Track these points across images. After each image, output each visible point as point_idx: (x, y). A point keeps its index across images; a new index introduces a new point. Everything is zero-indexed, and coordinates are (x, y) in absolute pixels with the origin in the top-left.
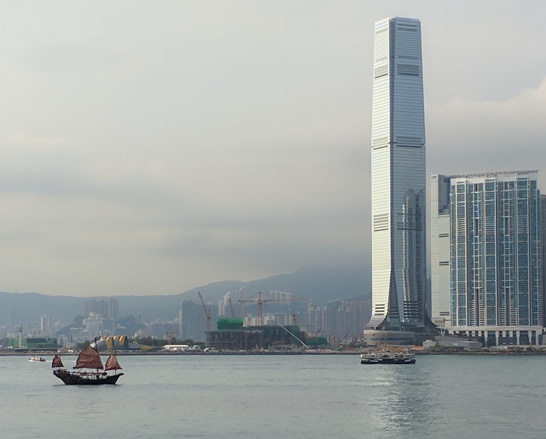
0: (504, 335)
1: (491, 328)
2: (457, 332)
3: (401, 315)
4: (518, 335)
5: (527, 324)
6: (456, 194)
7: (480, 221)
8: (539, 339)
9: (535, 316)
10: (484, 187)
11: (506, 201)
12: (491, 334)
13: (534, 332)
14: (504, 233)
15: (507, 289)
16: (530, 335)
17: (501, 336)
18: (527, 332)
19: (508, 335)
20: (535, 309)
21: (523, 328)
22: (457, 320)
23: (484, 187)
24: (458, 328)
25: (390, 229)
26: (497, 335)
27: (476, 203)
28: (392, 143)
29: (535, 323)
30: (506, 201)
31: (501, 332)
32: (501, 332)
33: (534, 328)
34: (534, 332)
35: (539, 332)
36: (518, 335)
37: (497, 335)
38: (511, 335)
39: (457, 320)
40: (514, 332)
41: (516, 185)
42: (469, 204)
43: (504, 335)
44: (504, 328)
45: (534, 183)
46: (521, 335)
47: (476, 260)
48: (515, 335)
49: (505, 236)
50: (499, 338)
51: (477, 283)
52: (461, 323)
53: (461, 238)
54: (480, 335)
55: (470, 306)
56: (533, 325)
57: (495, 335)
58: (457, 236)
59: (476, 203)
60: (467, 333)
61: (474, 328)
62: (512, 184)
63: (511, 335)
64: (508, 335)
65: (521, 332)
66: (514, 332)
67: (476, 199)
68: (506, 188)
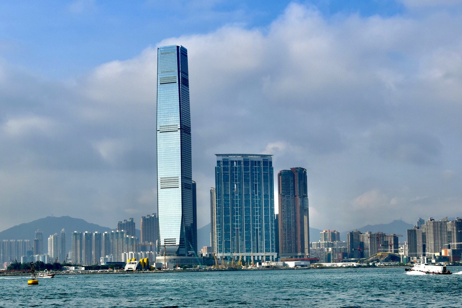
0: (256, 259)
1: (248, 254)
5: (269, 252)
9: (272, 246)
13: (273, 256)
15: (257, 229)
17: (254, 259)
18: (269, 256)
19: (258, 259)
21: (268, 254)
25: (180, 188)
27: (236, 173)
28: (181, 129)
29: (273, 251)
31: (254, 257)
34: (273, 256)
35: (275, 256)
40: (262, 256)
41: (262, 163)
43: (256, 259)
44: (256, 254)
45: (271, 163)
53: (226, 195)
62: (259, 162)
64: (258, 259)
65: (266, 256)
66: (262, 256)
67: (236, 171)
68: (255, 165)
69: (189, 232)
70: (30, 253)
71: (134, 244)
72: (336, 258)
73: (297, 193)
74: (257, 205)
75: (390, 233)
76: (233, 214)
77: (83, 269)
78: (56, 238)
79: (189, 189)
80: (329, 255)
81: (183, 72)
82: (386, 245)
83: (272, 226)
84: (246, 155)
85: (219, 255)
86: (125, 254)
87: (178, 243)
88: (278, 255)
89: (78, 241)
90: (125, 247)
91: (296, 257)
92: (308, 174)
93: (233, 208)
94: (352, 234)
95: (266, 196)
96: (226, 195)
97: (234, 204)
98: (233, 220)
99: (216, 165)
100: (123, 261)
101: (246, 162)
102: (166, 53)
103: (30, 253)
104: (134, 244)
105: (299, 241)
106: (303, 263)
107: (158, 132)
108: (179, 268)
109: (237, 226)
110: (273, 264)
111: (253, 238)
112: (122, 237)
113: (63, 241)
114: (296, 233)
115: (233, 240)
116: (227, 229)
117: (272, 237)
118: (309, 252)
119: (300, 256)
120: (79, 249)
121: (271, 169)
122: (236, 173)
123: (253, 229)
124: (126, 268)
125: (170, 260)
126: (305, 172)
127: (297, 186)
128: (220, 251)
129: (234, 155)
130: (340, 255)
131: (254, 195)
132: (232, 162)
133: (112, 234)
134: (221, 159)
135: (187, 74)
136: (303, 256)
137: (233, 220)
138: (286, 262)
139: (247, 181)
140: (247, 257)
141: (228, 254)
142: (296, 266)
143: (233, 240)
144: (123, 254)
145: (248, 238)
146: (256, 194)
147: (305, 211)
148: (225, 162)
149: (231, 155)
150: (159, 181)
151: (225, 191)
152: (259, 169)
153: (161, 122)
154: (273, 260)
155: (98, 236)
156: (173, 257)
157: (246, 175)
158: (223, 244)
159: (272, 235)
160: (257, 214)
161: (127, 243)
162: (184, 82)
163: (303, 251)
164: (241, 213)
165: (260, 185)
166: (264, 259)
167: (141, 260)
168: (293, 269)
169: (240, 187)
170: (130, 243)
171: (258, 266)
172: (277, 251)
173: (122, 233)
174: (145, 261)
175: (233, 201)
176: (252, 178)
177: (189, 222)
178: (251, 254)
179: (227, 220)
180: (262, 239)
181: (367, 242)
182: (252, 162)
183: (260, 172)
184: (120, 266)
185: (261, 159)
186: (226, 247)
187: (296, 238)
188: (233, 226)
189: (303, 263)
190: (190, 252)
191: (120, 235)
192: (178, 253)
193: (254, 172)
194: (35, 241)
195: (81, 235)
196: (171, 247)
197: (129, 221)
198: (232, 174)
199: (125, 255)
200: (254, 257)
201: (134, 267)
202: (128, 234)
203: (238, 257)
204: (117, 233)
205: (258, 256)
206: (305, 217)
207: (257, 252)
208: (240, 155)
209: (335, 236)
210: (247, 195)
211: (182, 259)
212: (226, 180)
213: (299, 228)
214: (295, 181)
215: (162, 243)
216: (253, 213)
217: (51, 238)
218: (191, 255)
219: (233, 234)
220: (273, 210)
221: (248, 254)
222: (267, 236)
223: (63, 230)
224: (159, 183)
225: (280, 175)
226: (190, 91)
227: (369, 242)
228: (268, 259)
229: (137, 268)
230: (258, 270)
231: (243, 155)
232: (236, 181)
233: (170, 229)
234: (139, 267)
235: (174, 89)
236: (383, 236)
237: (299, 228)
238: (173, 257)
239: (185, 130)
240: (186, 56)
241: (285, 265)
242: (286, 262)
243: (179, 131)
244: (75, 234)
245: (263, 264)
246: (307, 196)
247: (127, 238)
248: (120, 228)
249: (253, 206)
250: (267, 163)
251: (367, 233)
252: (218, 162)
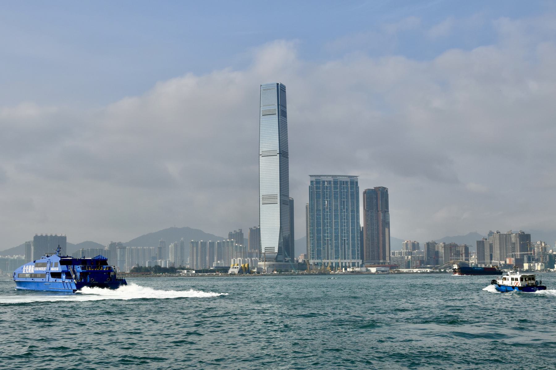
0: (344, 265)
1: (337, 261)
9: (358, 255)
12: (337, 265)
13: (358, 263)
17: (342, 265)
18: (355, 263)
19: (345, 265)
21: (353, 261)
24: (316, 261)
29: (358, 259)
31: (342, 263)
35: (360, 263)
41: (349, 183)
43: (344, 265)
44: (344, 261)
45: (357, 183)
52: (319, 258)
62: (347, 182)
64: (345, 265)
67: (327, 189)
69: (287, 243)
70: (154, 258)
71: (242, 251)
72: (415, 265)
73: (380, 209)
75: (461, 243)
76: (324, 226)
77: (194, 272)
78: (176, 246)
79: (287, 206)
80: (409, 262)
81: (282, 105)
82: (458, 254)
83: (357, 237)
84: (335, 176)
85: (311, 262)
86: (234, 260)
87: (276, 250)
88: (363, 261)
89: (195, 248)
90: (235, 253)
91: (379, 263)
92: (389, 192)
93: (324, 222)
94: (428, 244)
95: (353, 211)
96: (318, 210)
98: (324, 232)
99: (309, 184)
100: (227, 266)
101: (335, 182)
102: (268, 89)
103: (154, 258)
104: (242, 251)
105: (381, 250)
106: (383, 269)
107: (261, 156)
108: (275, 272)
109: (328, 237)
110: (357, 269)
111: (341, 247)
112: (232, 245)
113: (182, 248)
114: (378, 243)
115: (324, 248)
116: (319, 239)
117: (358, 247)
118: (390, 260)
119: (382, 263)
120: (195, 254)
121: (357, 188)
123: (342, 239)
124: (230, 272)
125: (270, 266)
126: (387, 191)
127: (380, 202)
128: (313, 258)
129: (325, 176)
130: (418, 262)
132: (324, 182)
133: (224, 242)
134: (314, 179)
135: (285, 107)
136: (385, 263)
137: (324, 232)
138: (369, 268)
139: (336, 198)
141: (319, 261)
142: (377, 271)
143: (324, 248)
144: (232, 260)
145: (337, 247)
147: (386, 224)
148: (318, 182)
149: (323, 176)
150: (261, 198)
151: (317, 206)
152: (347, 188)
153: (264, 148)
154: (358, 267)
155: (212, 244)
156: (272, 263)
157: (336, 193)
158: (315, 252)
159: (358, 244)
160: (345, 226)
161: (236, 250)
162: (282, 113)
163: (384, 258)
164: (331, 227)
165: (347, 202)
166: (351, 265)
167: (242, 265)
168: (374, 274)
169: (330, 203)
170: (238, 250)
171: (344, 271)
172: (362, 258)
173: (232, 242)
174: (246, 266)
175: (324, 215)
176: (341, 195)
177: (287, 233)
178: (339, 261)
179: (319, 232)
180: (349, 248)
181: (442, 251)
182: (341, 181)
183: (348, 190)
184: (225, 270)
185: (348, 180)
186: (317, 255)
187: (378, 247)
188: (324, 236)
189: (383, 269)
190: (287, 259)
191: (230, 244)
192: (276, 259)
194: (159, 248)
195: (197, 243)
196: (271, 254)
197: (238, 231)
198: (323, 192)
199: (234, 260)
200: (342, 263)
201: (236, 271)
202: (236, 243)
203: (328, 263)
204: (228, 242)
205: (346, 263)
206: (387, 230)
208: (330, 176)
209: (415, 246)
210: (336, 210)
211: (280, 265)
212: (318, 197)
213: (381, 238)
214: (378, 199)
215: (263, 251)
216: (341, 226)
217: (171, 246)
218: (288, 261)
219: (324, 244)
220: (358, 223)
221: (337, 261)
222: (353, 246)
223: (182, 239)
224: (261, 199)
225: (365, 193)
226: (288, 121)
227: (443, 251)
228: (354, 265)
229: (239, 272)
230: (344, 274)
231: (333, 176)
232: (327, 198)
233: (270, 240)
234: (241, 271)
235: (274, 120)
236: (455, 246)
237: (381, 238)
238: (272, 263)
239: (284, 154)
240: (285, 92)
241: (367, 270)
242: (369, 268)
243: (278, 155)
244: (192, 242)
245: (348, 270)
246: (388, 211)
247: (236, 247)
248: (230, 238)
249: (341, 219)
250: (353, 183)
251: (441, 244)
252: (312, 182)
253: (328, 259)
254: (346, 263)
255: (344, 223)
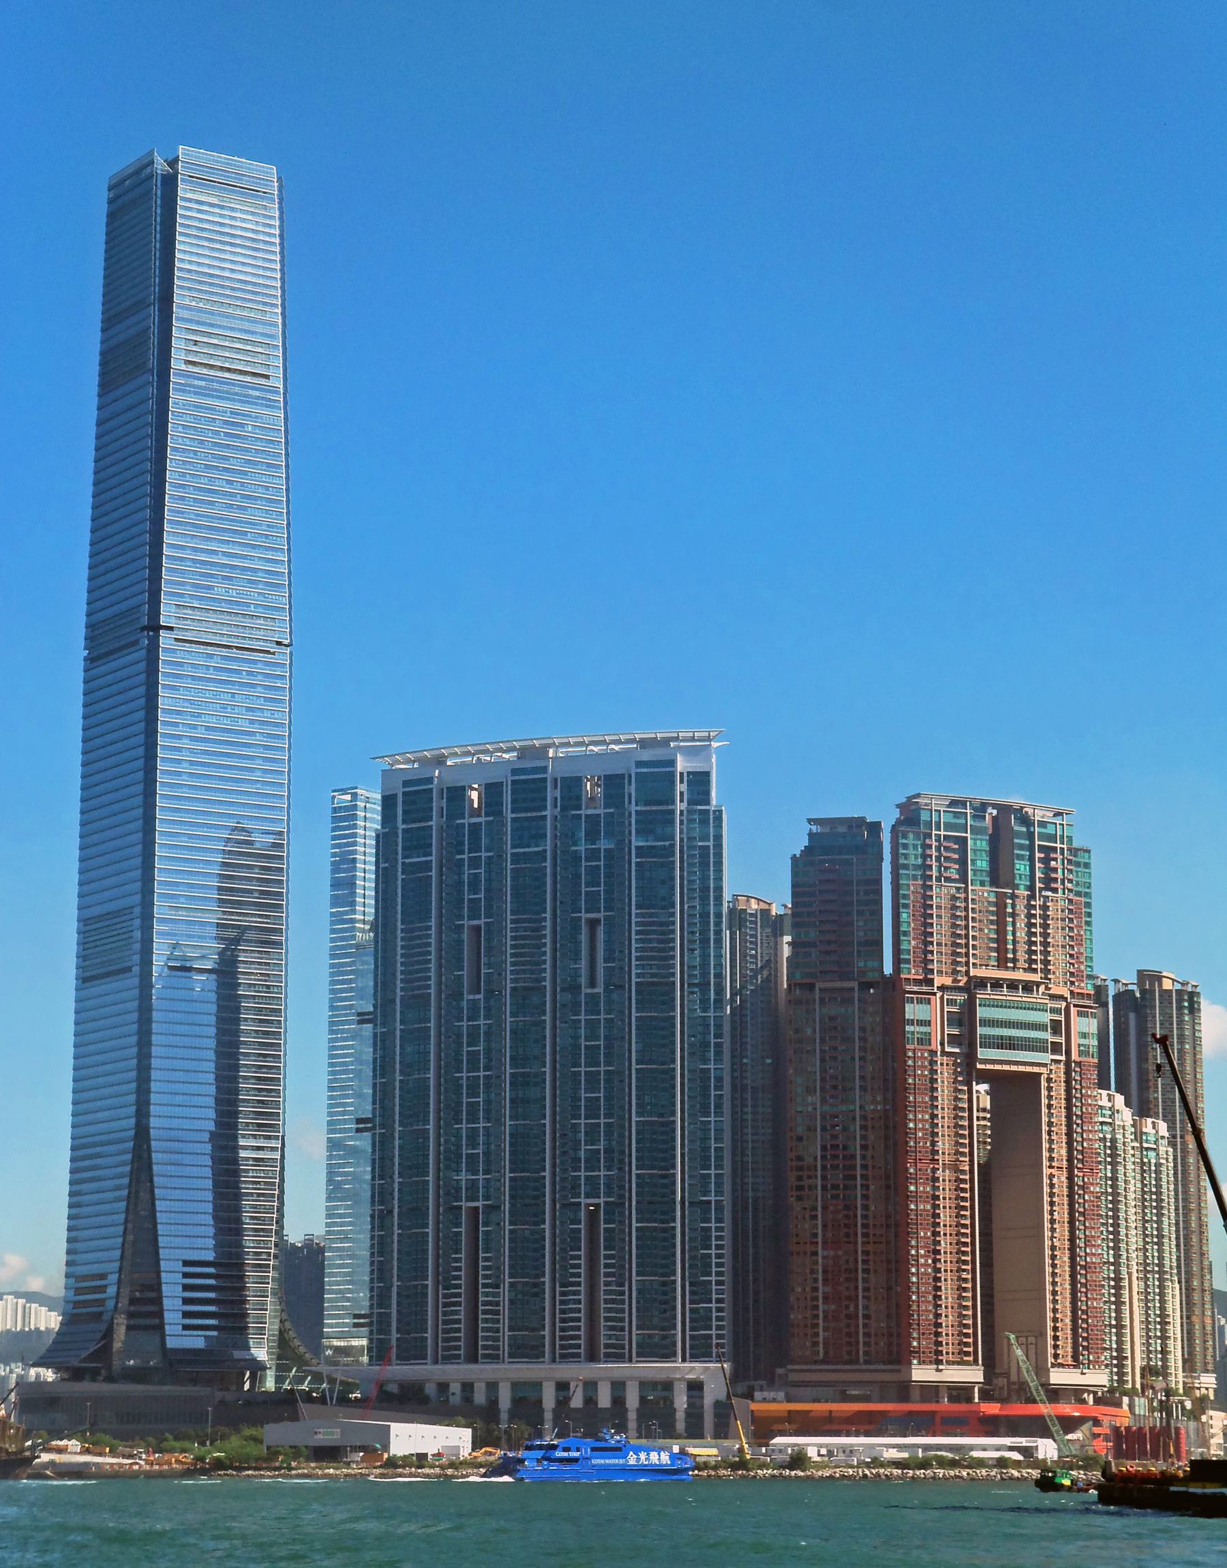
1: (526, 1370)
2: (393, 1388)
3: (173, 1317)
4: (632, 1400)
5: (669, 1355)
6: (401, 826)
7: (488, 932)
8: (716, 1415)
9: (700, 1320)
10: (508, 797)
11: (593, 855)
13: (695, 1387)
14: (583, 980)
16: (681, 1401)
17: (562, 1403)
19: (590, 1401)
20: (700, 1292)
22: (395, 1335)
23: (508, 797)
26: (549, 1399)
29: (700, 1351)
30: (593, 855)
31: (562, 1386)
32: (562, 1386)
33: (695, 1369)
35: (715, 1391)
36: (632, 1400)
37: (549, 1399)
38: (604, 1401)
39: (395, 1335)
42: (451, 865)
43: (577, 1402)
44: (578, 1372)
45: (700, 781)
46: (643, 1400)
47: (473, 1092)
48: (619, 1401)
49: (585, 990)
50: (555, 1411)
51: (472, 1186)
52: (412, 1352)
53: (416, 1002)
54: (480, 1397)
55: (445, 1280)
56: (695, 1357)
57: (540, 1401)
58: (399, 993)
59: (475, 863)
60: (431, 1389)
61: (456, 1372)
63: (604, 1401)
64: (590, 1401)
66: (618, 1387)
67: (475, 847)
74: (592, 1051)
96: (416, 1002)
97: (458, 1053)
122: (475, 863)
131: (574, 988)
140: (516, 1386)
146: (592, 984)
152: (615, 826)
188: (452, 1192)
193: (582, 848)
207: (592, 1357)
253: (473, 1358)
254: (591, 1386)
255: (473, 1090)
